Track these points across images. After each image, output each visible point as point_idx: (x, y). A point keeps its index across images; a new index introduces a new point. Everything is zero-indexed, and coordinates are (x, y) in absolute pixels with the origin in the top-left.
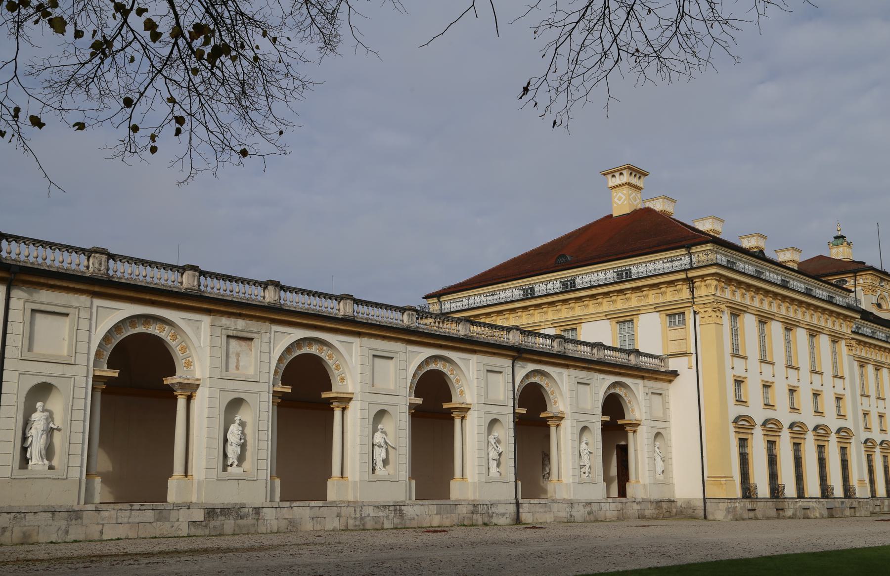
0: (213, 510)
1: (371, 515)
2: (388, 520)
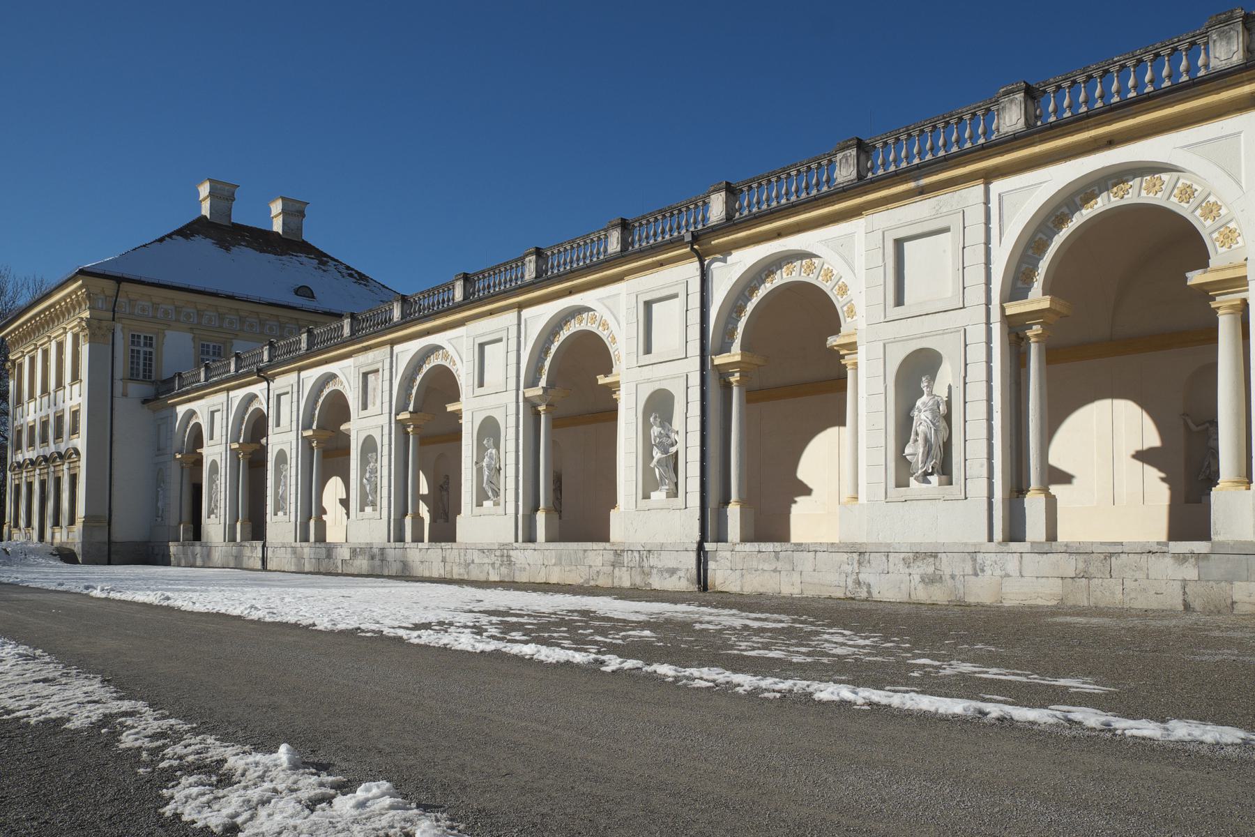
1: (475, 562)
2: (494, 568)
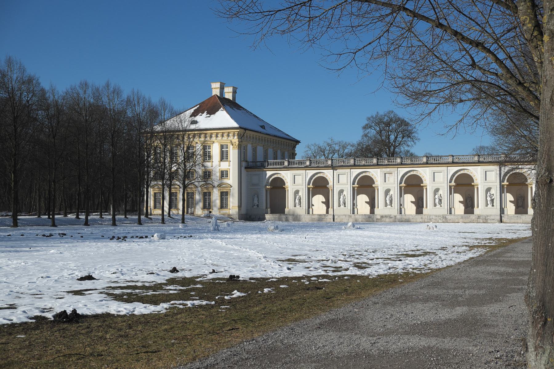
0: (383, 216)
